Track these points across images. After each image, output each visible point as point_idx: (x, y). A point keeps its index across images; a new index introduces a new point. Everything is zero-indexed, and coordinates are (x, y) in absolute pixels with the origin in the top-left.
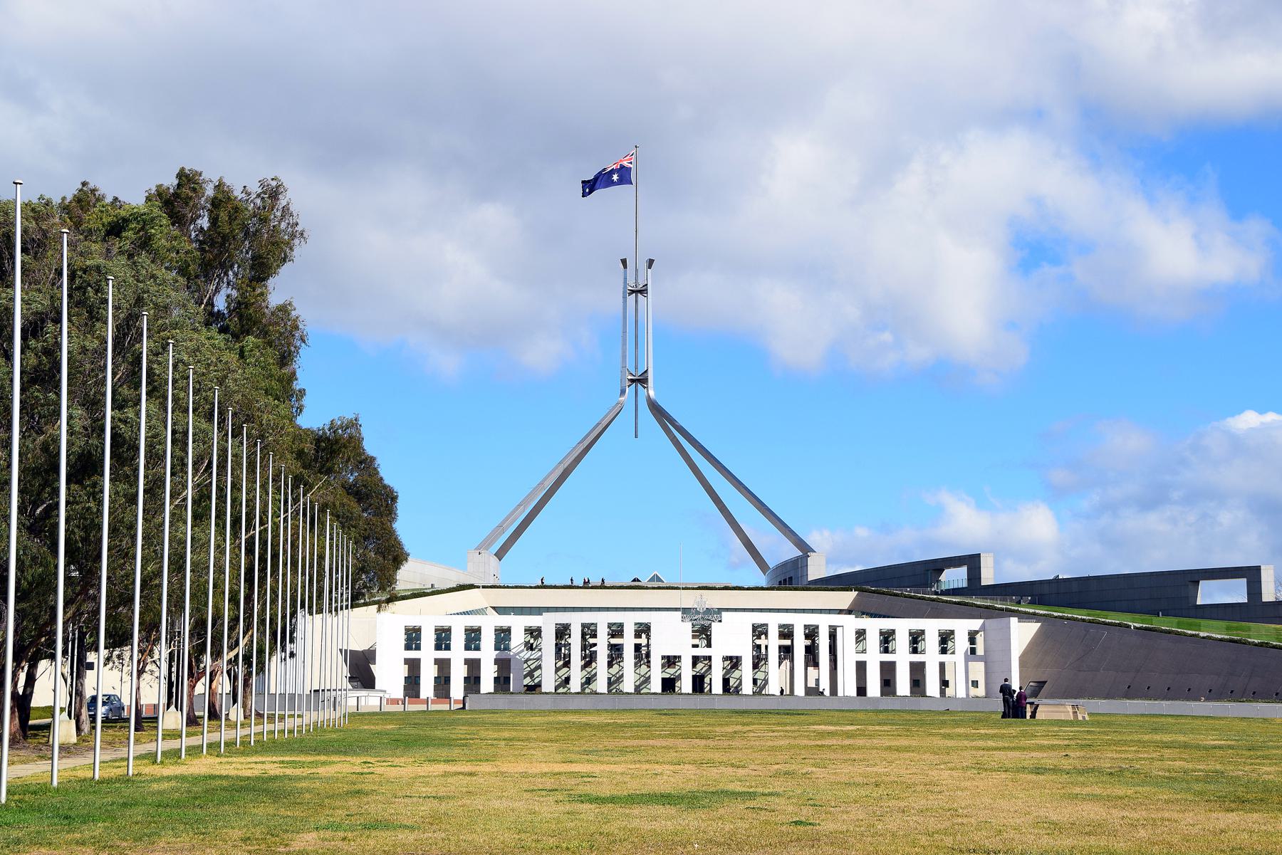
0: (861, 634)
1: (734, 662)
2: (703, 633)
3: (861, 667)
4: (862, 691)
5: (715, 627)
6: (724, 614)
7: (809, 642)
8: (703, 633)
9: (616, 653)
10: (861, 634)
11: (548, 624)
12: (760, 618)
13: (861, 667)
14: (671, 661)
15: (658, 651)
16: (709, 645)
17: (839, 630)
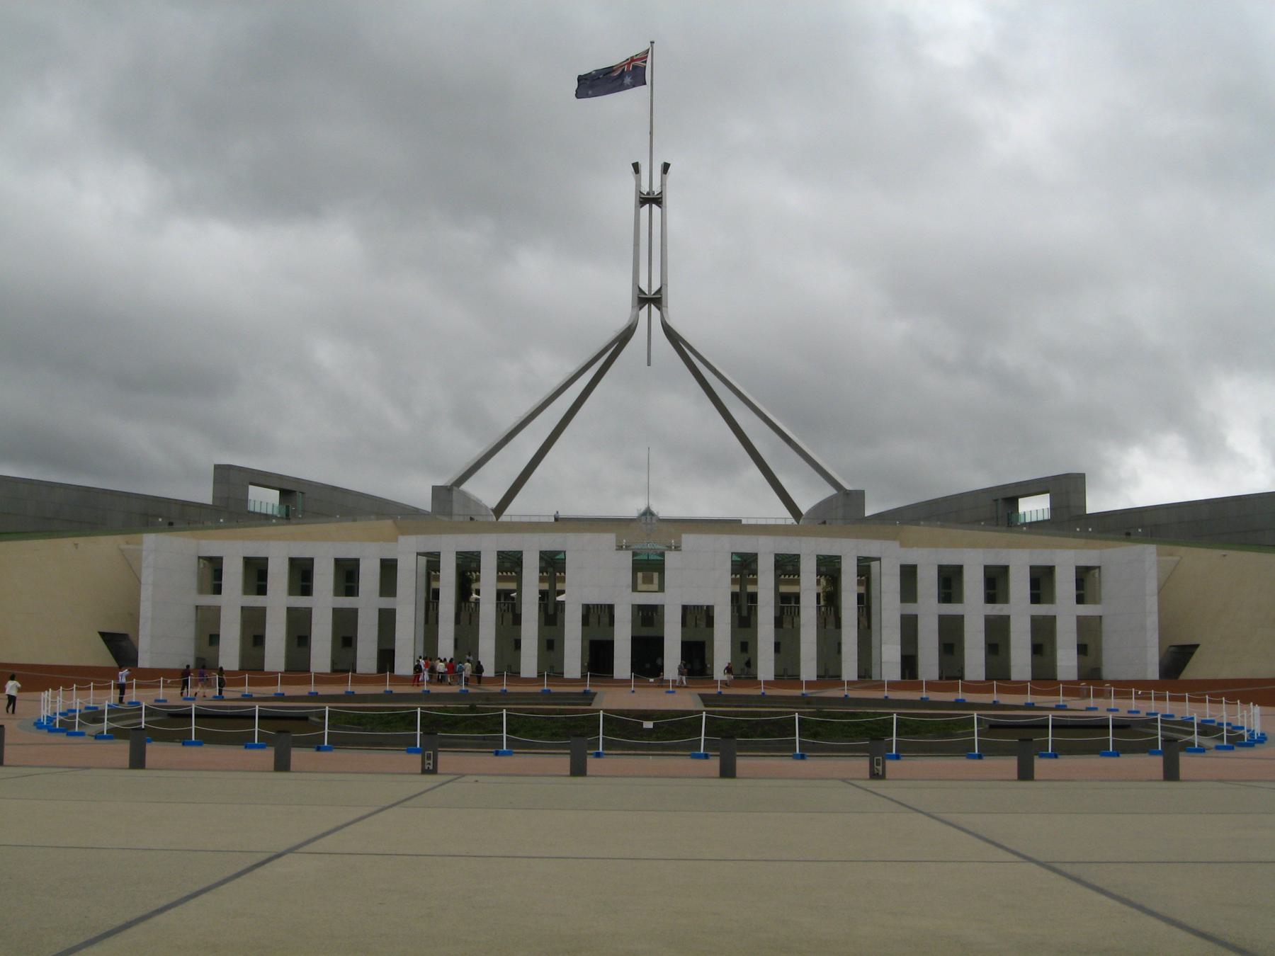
0: (909, 574)
1: (698, 617)
2: (648, 568)
3: (909, 626)
4: (909, 663)
5: (671, 559)
6: (689, 540)
7: (862, 590)
8: (648, 568)
9: (509, 605)
10: (909, 574)
11: (407, 552)
12: (745, 544)
13: (909, 626)
14: (598, 616)
15: (573, 600)
16: (661, 588)
17: (874, 565)
